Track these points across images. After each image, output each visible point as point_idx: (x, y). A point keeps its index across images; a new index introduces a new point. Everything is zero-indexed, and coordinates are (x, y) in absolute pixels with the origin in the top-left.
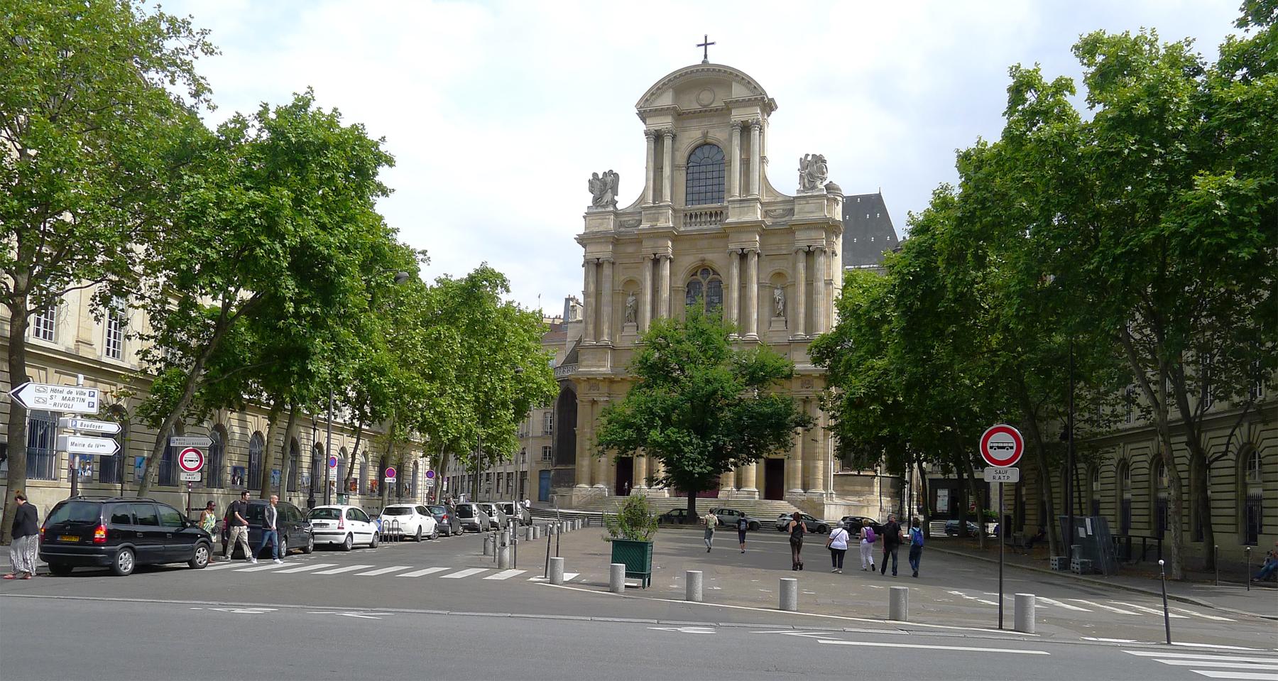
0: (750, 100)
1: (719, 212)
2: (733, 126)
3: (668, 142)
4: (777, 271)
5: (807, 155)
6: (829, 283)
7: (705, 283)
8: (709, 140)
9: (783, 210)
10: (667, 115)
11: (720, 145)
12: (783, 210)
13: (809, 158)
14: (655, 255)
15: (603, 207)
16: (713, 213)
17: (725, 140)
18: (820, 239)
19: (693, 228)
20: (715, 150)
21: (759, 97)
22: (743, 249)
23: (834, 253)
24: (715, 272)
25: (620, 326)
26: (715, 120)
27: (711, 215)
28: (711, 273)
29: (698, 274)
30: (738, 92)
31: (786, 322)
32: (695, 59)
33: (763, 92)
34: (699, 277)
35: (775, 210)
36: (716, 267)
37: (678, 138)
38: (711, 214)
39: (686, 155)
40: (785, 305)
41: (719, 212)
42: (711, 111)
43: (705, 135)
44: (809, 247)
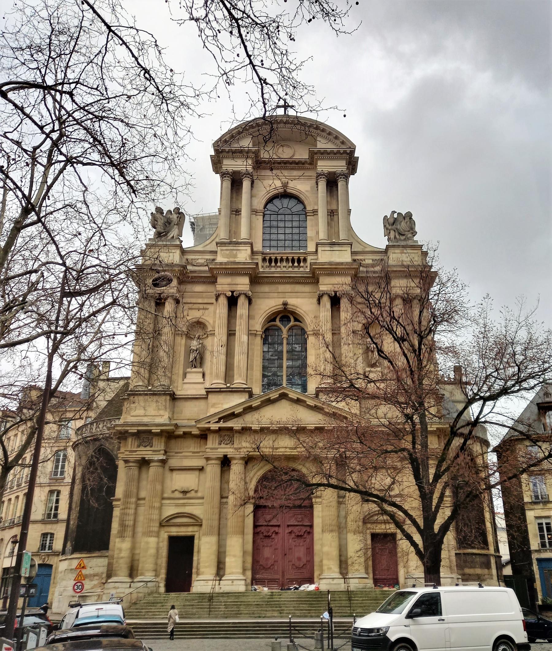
0: (338, 152)
1: (302, 258)
2: (319, 176)
3: (246, 184)
5: (394, 212)
7: (285, 330)
8: (289, 191)
9: (373, 260)
11: (301, 196)
12: (373, 260)
13: (395, 216)
14: (232, 292)
16: (296, 258)
17: (307, 191)
20: (293, 202)
25: (181, 372)
26: (295, 173)
27: (293, 261)
28: (292, 319)
34: (278, 323)
39: (264, 202)
41: (302, 258)
43: (285, 185)
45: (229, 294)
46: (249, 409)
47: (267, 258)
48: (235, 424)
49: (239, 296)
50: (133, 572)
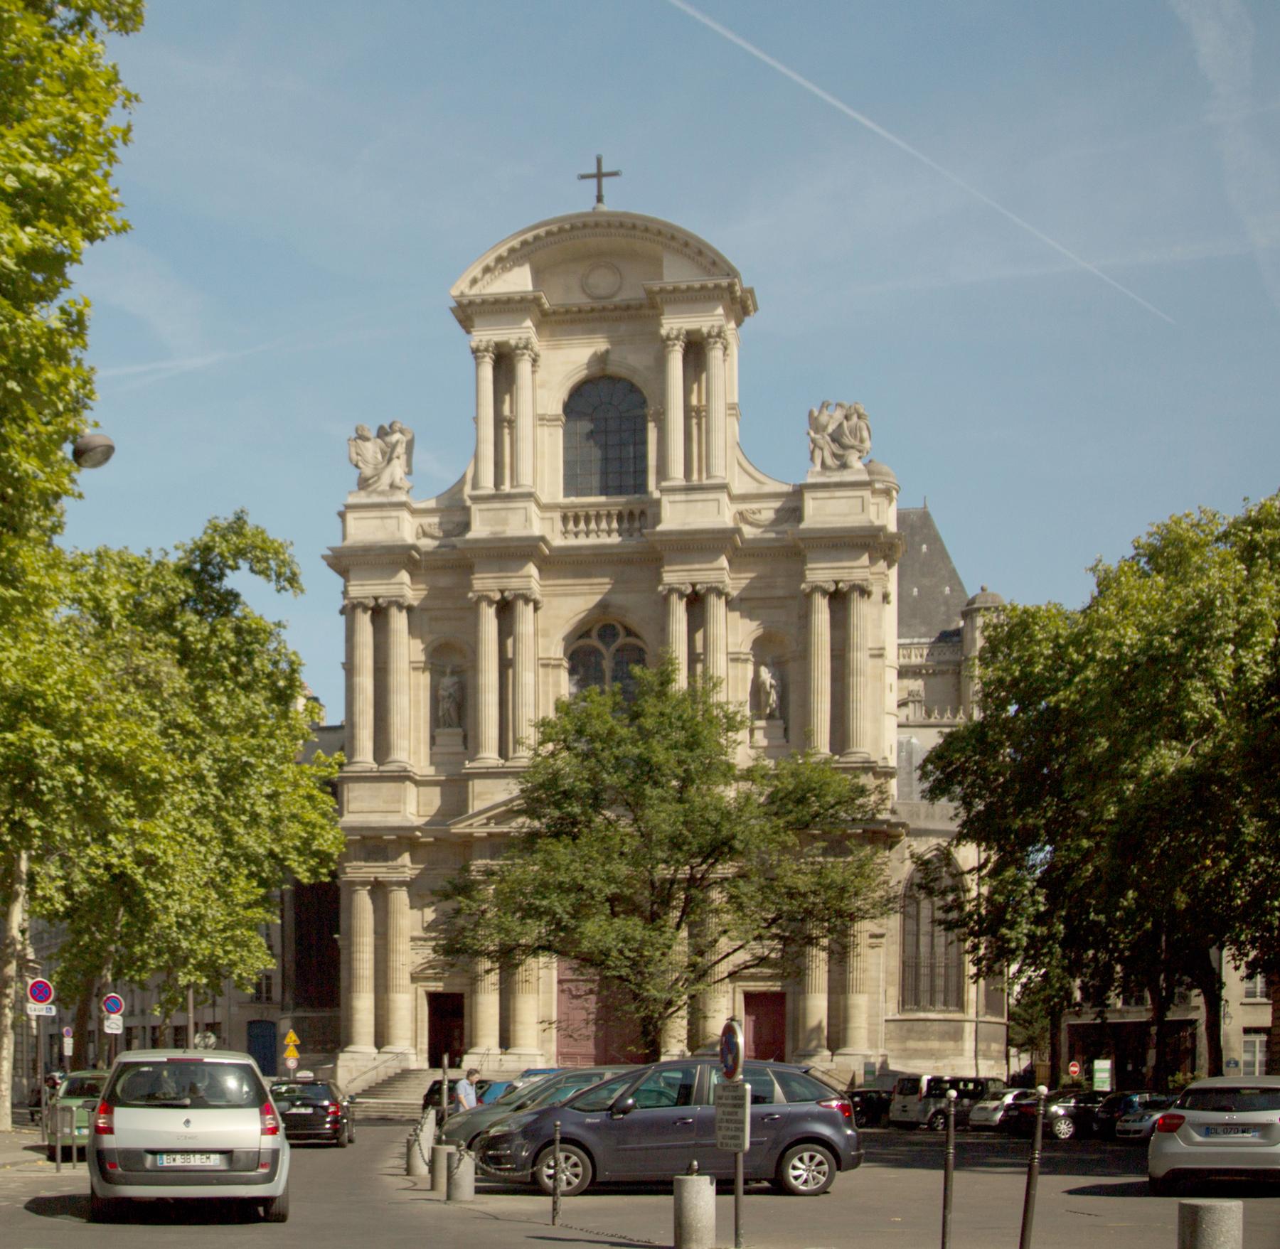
1: (637, 512)
6: (879, 654)
15: (382, 493)
18: (858, 569)
19: (582, 541)
21: (724, 282)
22: (694, 585)
23: (885, 598)
24: (629, 632)
28: (622, 632)
29: (594, 633)
30: (677, 273)
31: (786, 730)
32: (579, 201)
33: (731, 272)
34: (594, 641)
36: (633, 621)
37: (541, 362)
38: (631, 514)
40: (783, 697)
41: (637, 512)
42: (616, 308)
44: (836, 583)
50: (381, 1039)
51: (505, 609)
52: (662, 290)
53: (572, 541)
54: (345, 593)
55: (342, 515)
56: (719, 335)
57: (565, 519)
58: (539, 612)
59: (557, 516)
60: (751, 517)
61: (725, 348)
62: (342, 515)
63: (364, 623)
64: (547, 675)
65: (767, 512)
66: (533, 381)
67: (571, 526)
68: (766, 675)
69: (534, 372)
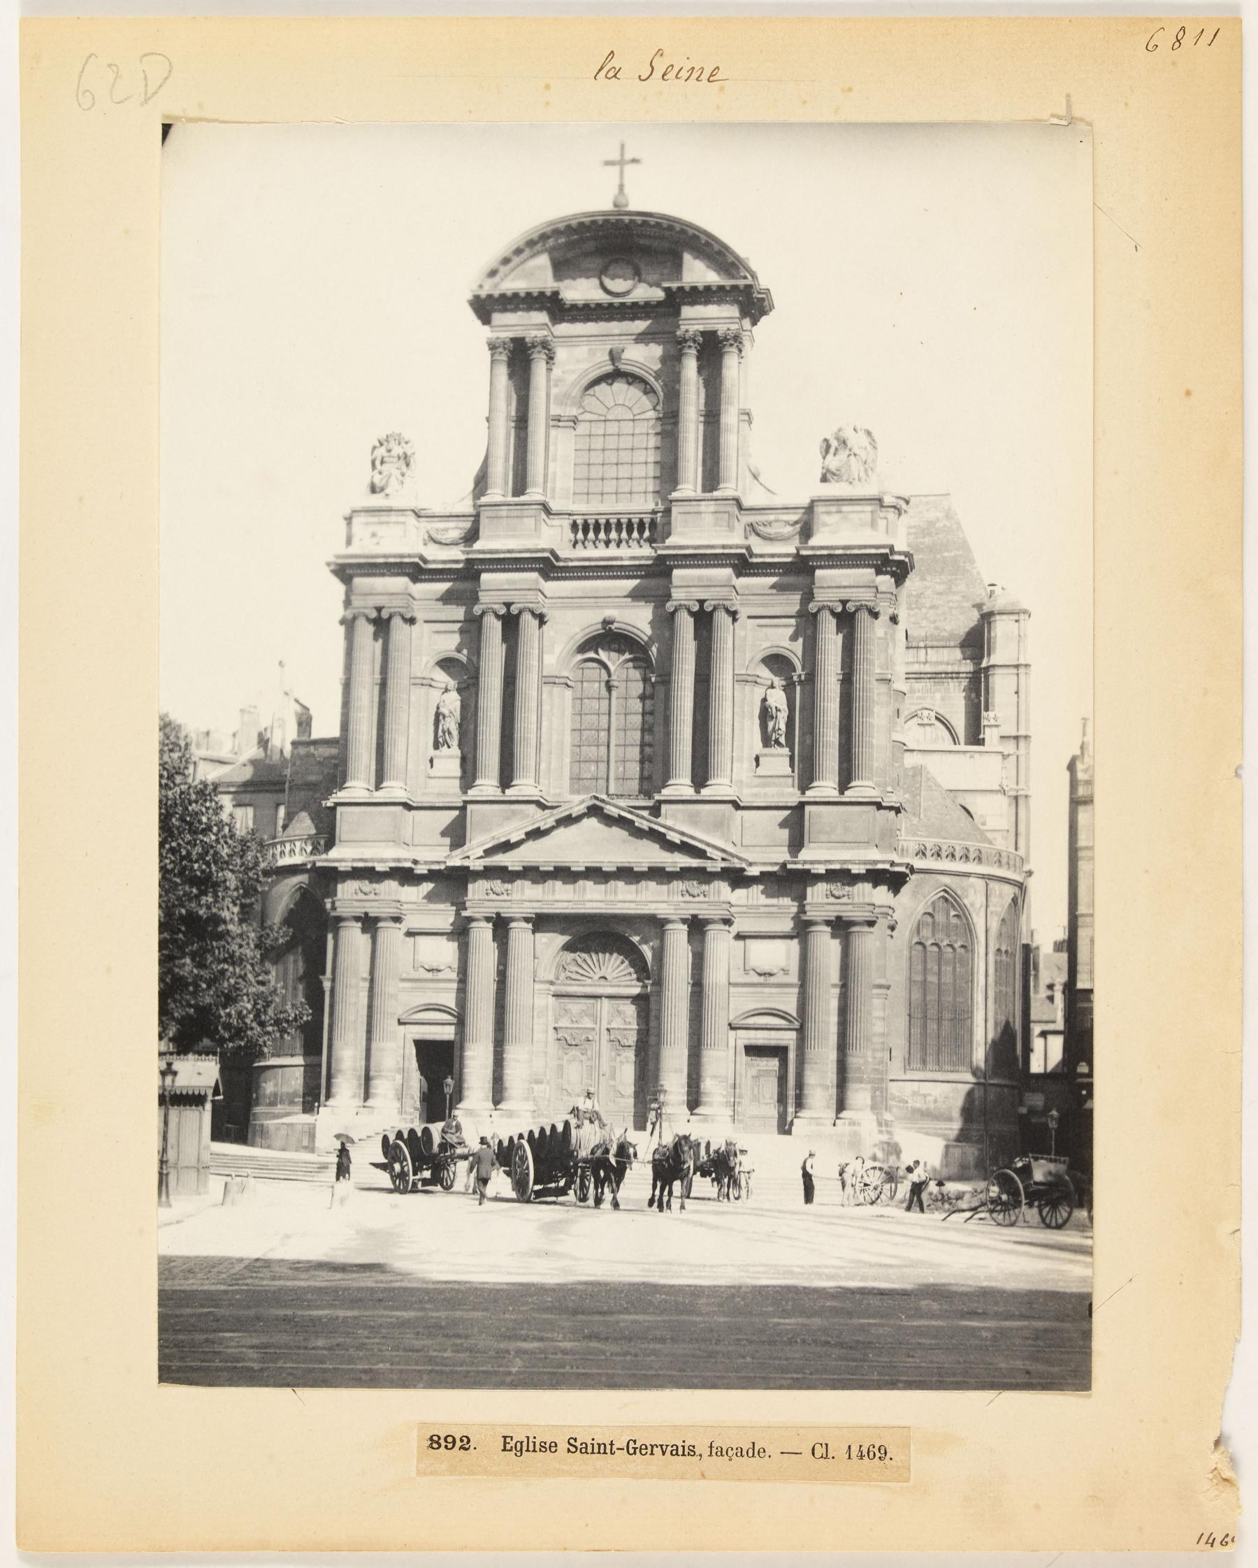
4: (775, 651)
10: (540, 309)
30: (697, 272)
35: (770, 523)
45: (503, 611)
46: (536, 834)
47: (580, 522)
48: (511, 860)
49: (520, 613)
51: (511, 623)
52: (681, 289)
53: (580, 552)
54: (348, 603)
55: (349, 520)
56: (737, 338)
57: (574, 526)
58: (545, 627)
59: (566, 523)
60: (761, 529)
61: (740, 351)
62: (349, 520)
63: (365, 630)
64: (551, 693)
65: (784, 526)
66: (548, 380)
67: (580, 535)
68: (778, 699)
69: (549, 370)
